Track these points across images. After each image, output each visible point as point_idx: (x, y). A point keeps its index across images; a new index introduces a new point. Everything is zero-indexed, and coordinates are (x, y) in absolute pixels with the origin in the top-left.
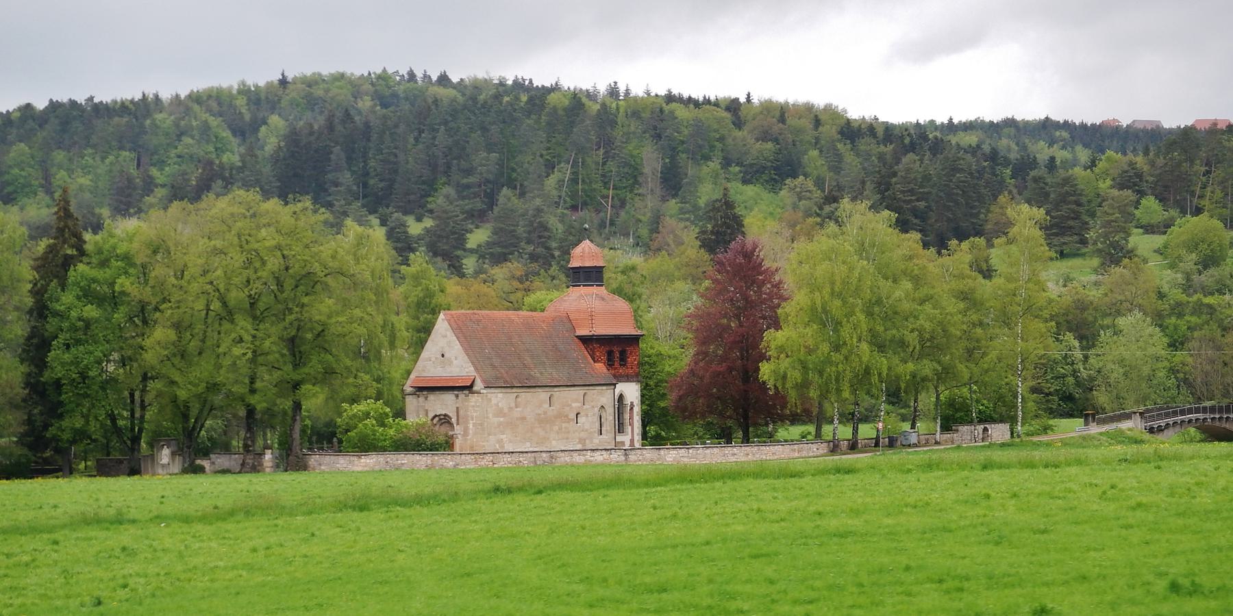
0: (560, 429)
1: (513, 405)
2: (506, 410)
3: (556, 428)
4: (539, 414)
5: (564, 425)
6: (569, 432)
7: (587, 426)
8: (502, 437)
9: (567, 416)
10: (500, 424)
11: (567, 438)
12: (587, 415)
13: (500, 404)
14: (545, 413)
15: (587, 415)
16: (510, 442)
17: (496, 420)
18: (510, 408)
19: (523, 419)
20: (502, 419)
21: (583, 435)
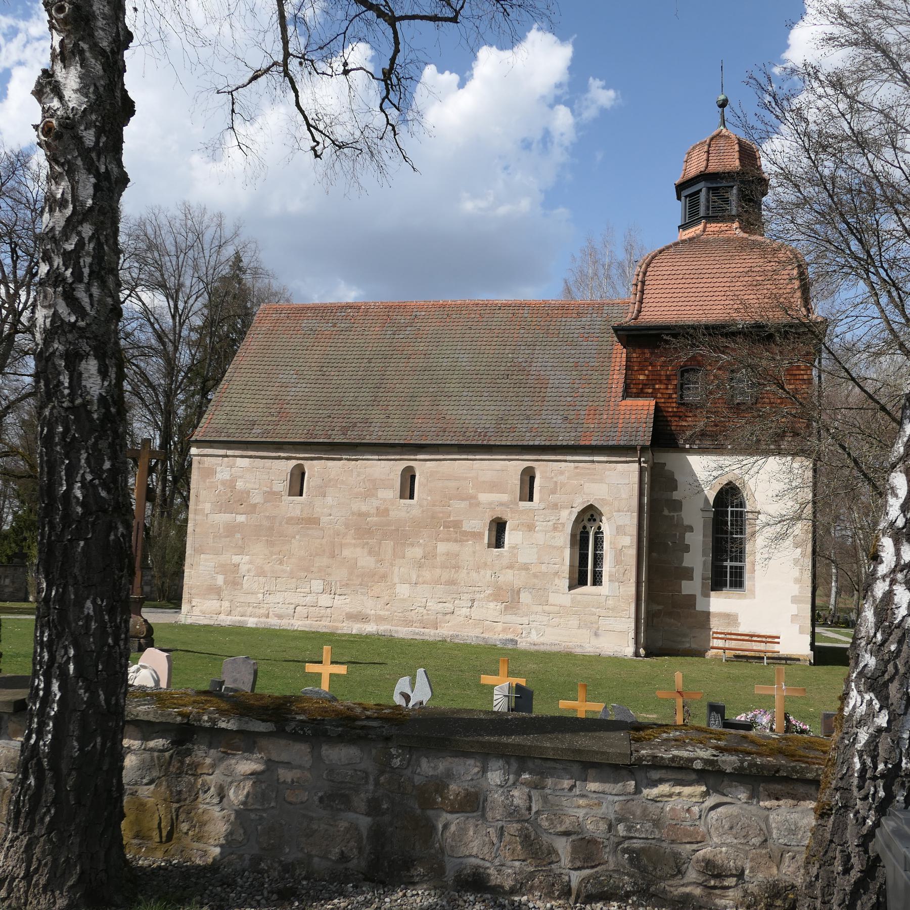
0: (429, 556)
1: (282, 486)
2: (256, 498)
3: (416, 552)
4: (362, 515)
5: (442, 547)
6: (457, 567)
7: (527, 556)
8: (236, 559)
9: (457, 524)
10: (231, 530)
11: (452, 582)
12: (531, 528)
13: (240, 485)
14: (383, 512)
15: (531, 528)
16: (261, 573)
17: (223, 518)
18: (271, 496)
19: (312, 521)
20: (241, 518)
21: (508, 577)
